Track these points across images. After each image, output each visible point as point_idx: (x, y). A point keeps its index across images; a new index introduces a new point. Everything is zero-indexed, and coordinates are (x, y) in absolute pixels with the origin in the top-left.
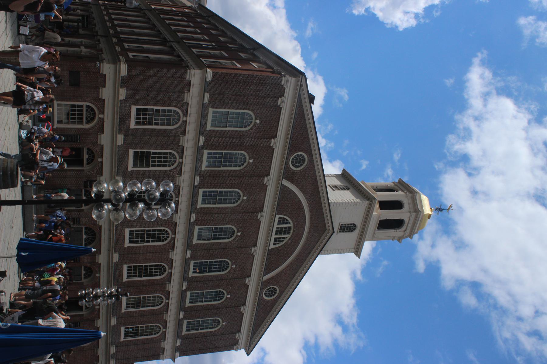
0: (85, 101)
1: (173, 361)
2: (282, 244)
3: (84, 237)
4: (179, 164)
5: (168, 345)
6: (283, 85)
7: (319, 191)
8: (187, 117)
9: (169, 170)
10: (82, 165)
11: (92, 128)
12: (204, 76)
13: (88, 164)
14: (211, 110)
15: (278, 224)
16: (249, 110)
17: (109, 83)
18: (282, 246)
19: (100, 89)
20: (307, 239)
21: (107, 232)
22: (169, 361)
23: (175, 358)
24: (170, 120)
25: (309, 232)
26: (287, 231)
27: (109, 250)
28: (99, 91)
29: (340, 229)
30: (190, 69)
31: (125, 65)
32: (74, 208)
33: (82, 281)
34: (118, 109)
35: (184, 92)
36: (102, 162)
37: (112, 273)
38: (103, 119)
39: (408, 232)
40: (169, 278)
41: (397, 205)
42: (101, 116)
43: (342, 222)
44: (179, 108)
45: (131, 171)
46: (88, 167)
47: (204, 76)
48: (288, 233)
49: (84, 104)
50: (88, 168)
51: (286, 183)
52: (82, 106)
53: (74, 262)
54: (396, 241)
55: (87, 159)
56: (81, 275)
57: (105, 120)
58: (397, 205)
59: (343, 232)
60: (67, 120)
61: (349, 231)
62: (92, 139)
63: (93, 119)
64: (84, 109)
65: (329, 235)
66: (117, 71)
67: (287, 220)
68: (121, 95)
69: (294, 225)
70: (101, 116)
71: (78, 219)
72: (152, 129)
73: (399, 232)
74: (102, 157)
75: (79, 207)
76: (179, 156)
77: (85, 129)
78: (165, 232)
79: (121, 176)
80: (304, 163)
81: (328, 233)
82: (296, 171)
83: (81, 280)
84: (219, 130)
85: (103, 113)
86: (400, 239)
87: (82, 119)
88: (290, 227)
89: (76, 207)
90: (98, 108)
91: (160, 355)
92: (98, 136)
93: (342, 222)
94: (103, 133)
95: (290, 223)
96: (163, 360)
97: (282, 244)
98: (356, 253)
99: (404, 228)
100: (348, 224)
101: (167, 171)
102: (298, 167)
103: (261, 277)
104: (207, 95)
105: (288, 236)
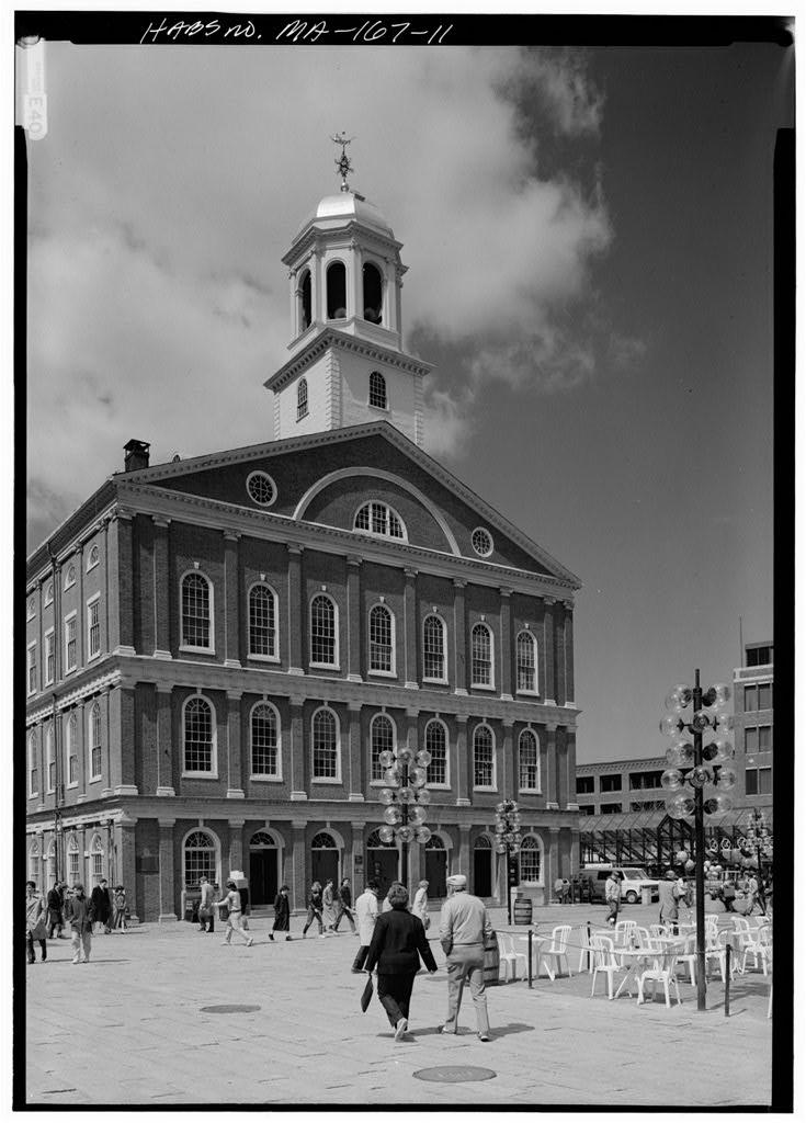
2: (401, 522)
15: (367, 528)
24: (202, 716)
26: (379, 509)
39: (390, 255)
41: (336, 272)
48: (384, 510)
52: (187, 853)
54: (404, 278)
58: (336, 272)
61: (384, 387)
64: (191, 849)
67: (361, 511)
69: (370, 498)
73: (388, 273)
80: (264, 479)
86: (401, 270)
87: (207, 854)
95: (367, 507)
97: (401, 522)
99: (382, 264)
100: (371, 389)
102: (270, 489)
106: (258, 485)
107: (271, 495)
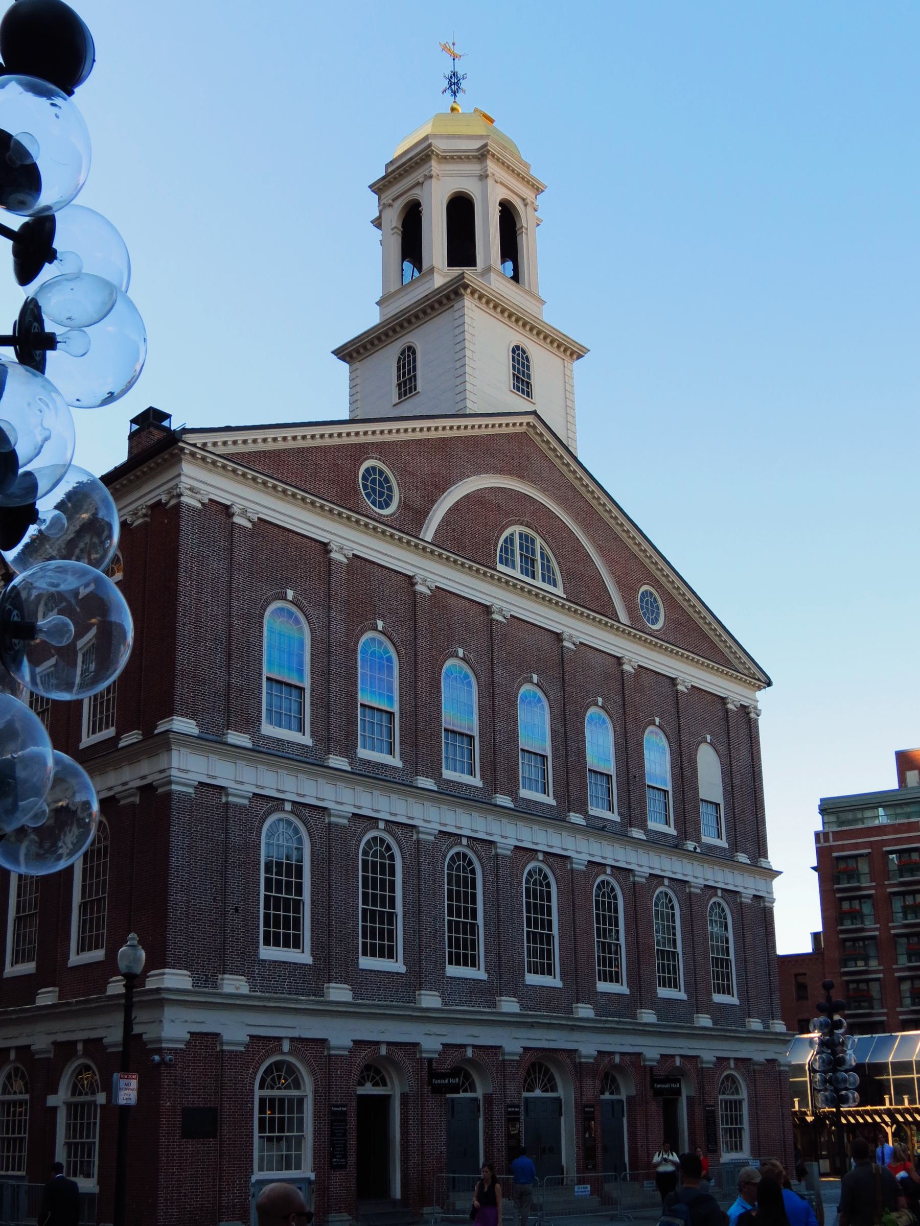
0: (252, 1091)
1: (778, 875)
3: (538, 1093)
4: (389, 832)
5: (746, 885)
6: (203, 504)
7: (443, 440)
8: (283, 800)
9: (403, 858)
10: (385, 1100)
11: (313, 1072)
12: (186, 740)
13: (385, 1085)
14: (267, 729)
16: (262, 616)
17: (209, 1022)
18: (559, 563)
19: (225, 1048)
20: (544, 490)
21: (537, 1034)
22: (776, 883)
23: (771, 870)
25: (532, 481)
27: (573, 1028)
28: (231, 1052)
29: (523, 393)
30: (170, 783)
31: (165, 976)
32: (481, 1120)
33: (624, 1100)
34: (303, 1000)
35: (224, 804)
36: (389, 1044)
37: (618, 1022)
38: (292, 1040)
40: (622, 872)
42: (286, 1046)
43: (510, 387)
44: (263, 821)
45: (405, 963)
46: (392, 1083)
47: (186, 740)
49: (258, 1093)
50: (396, 1082)
51: (428, 533)
52: (262, 1101)
53: (593, 1119)
55: (373, 1085)
56: (612, 1101)
57: (297, 1036)
59: (528, 384)
60: (284, 1143)
62: (339, 1072)
63: (291, 1070)
64: (268, 1093)
65: (540, 428)
66: (182, 1001)
67: (506, 541)
68: (237, 988)
70: (286, 1046)
71: (510, 1109)
72: (313, 901)
74: (377, 1043)
75: (479, 1106)
76: (372, 828)
77: (316, 1092)
78: (532, 877)
79: (417, 992)
80: (381, 473)
81: (534, 427)
82: (400, 499)
83: (621, 1101)
84: (312, 710)
85: (279, 1039)
87: (291, 1100)
88: (521, 535)
89: (478, 1117)
90: (268, 1055)
91: (765, 907)
92: (333, 1055)
93: (510, 387)
94: (323, 1041)
95: (512, 535)
96: (773, 901)
98: (575, 357)
101: (404, 863)
102: (390, 489)
103: (618, 628)
104: (235, 738)
105: (539, 541)
106: (373, 481)
107: (390, 498)
